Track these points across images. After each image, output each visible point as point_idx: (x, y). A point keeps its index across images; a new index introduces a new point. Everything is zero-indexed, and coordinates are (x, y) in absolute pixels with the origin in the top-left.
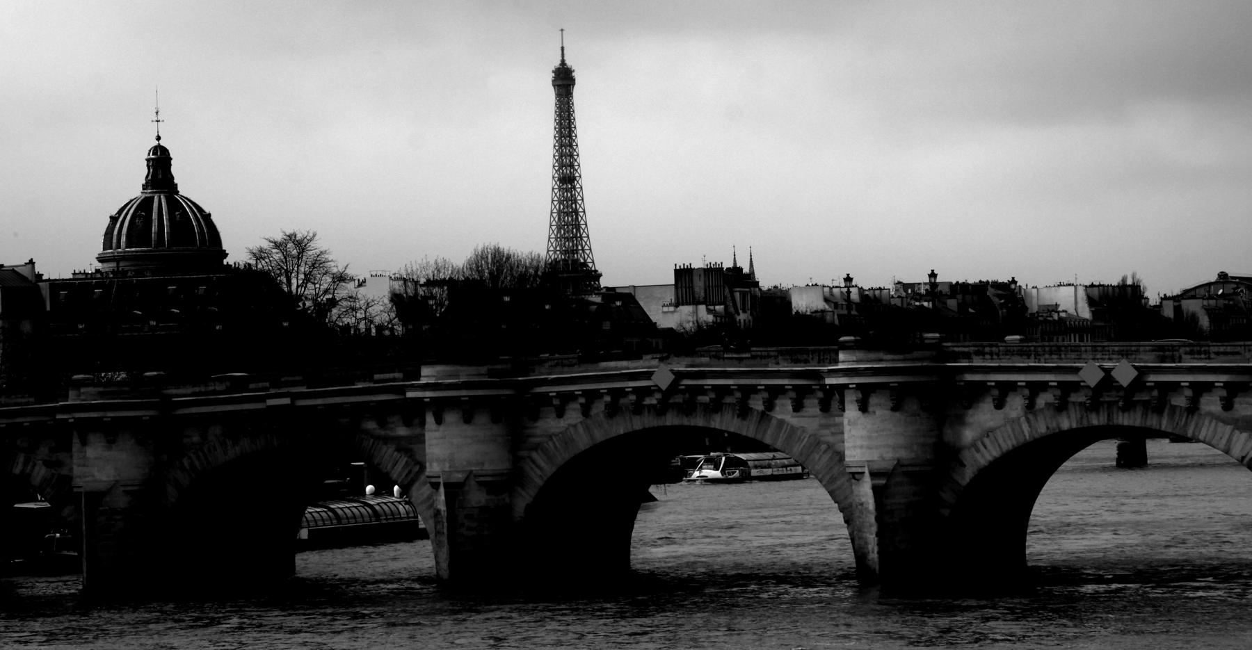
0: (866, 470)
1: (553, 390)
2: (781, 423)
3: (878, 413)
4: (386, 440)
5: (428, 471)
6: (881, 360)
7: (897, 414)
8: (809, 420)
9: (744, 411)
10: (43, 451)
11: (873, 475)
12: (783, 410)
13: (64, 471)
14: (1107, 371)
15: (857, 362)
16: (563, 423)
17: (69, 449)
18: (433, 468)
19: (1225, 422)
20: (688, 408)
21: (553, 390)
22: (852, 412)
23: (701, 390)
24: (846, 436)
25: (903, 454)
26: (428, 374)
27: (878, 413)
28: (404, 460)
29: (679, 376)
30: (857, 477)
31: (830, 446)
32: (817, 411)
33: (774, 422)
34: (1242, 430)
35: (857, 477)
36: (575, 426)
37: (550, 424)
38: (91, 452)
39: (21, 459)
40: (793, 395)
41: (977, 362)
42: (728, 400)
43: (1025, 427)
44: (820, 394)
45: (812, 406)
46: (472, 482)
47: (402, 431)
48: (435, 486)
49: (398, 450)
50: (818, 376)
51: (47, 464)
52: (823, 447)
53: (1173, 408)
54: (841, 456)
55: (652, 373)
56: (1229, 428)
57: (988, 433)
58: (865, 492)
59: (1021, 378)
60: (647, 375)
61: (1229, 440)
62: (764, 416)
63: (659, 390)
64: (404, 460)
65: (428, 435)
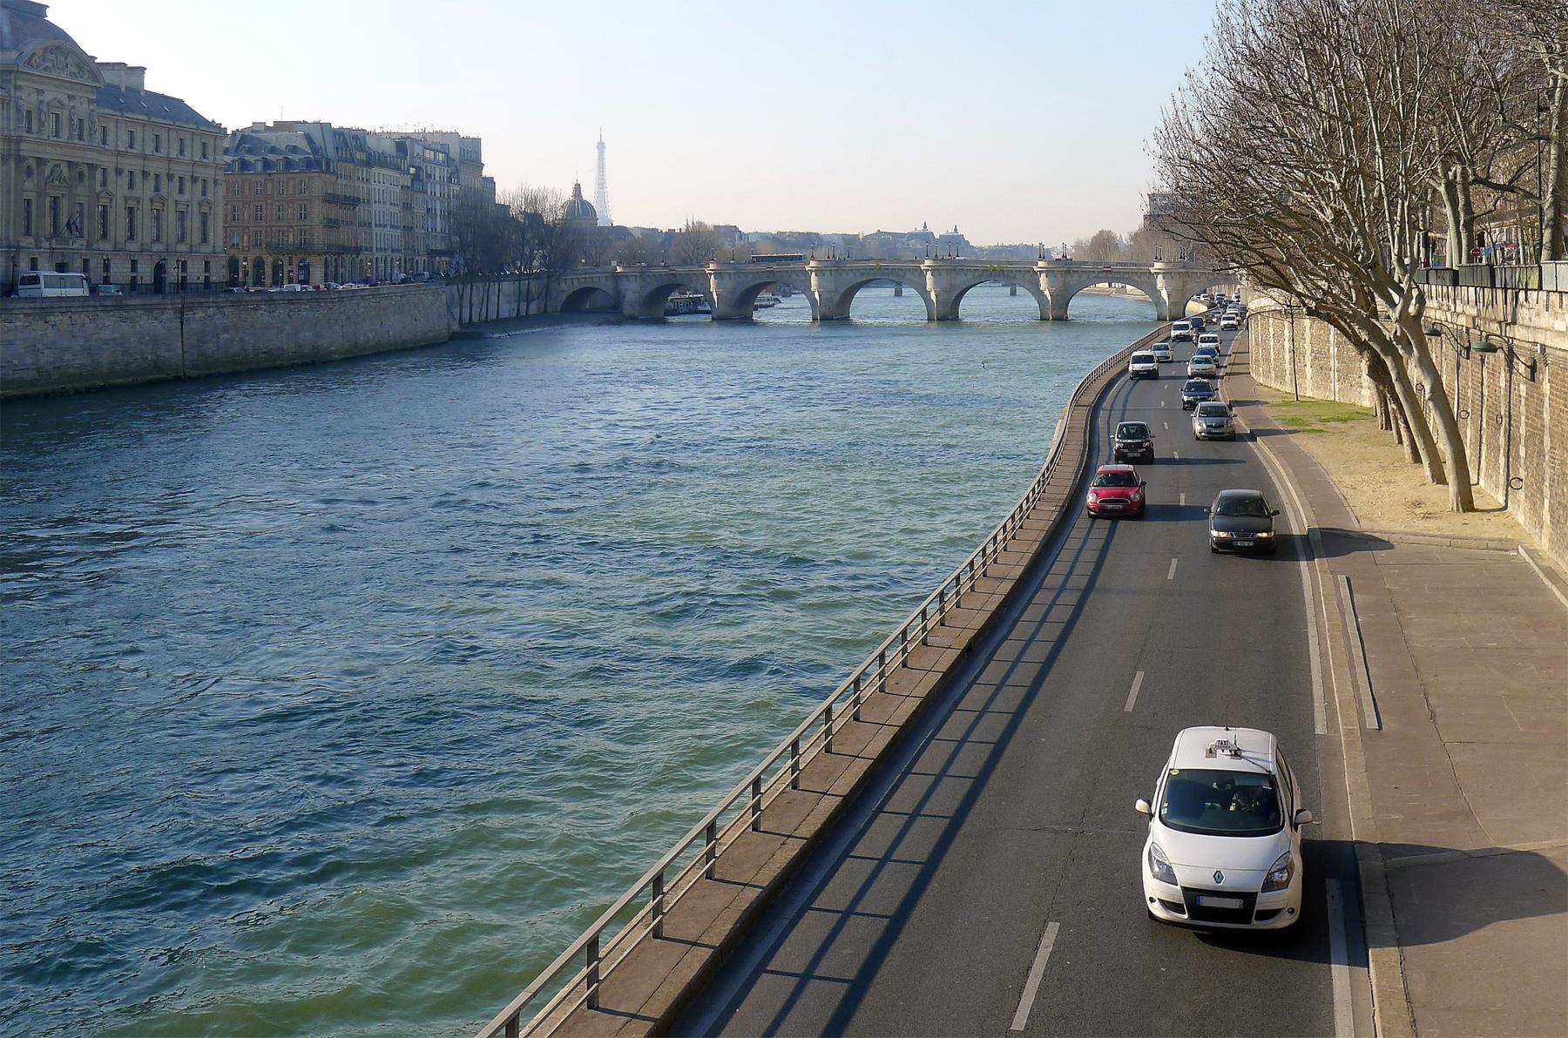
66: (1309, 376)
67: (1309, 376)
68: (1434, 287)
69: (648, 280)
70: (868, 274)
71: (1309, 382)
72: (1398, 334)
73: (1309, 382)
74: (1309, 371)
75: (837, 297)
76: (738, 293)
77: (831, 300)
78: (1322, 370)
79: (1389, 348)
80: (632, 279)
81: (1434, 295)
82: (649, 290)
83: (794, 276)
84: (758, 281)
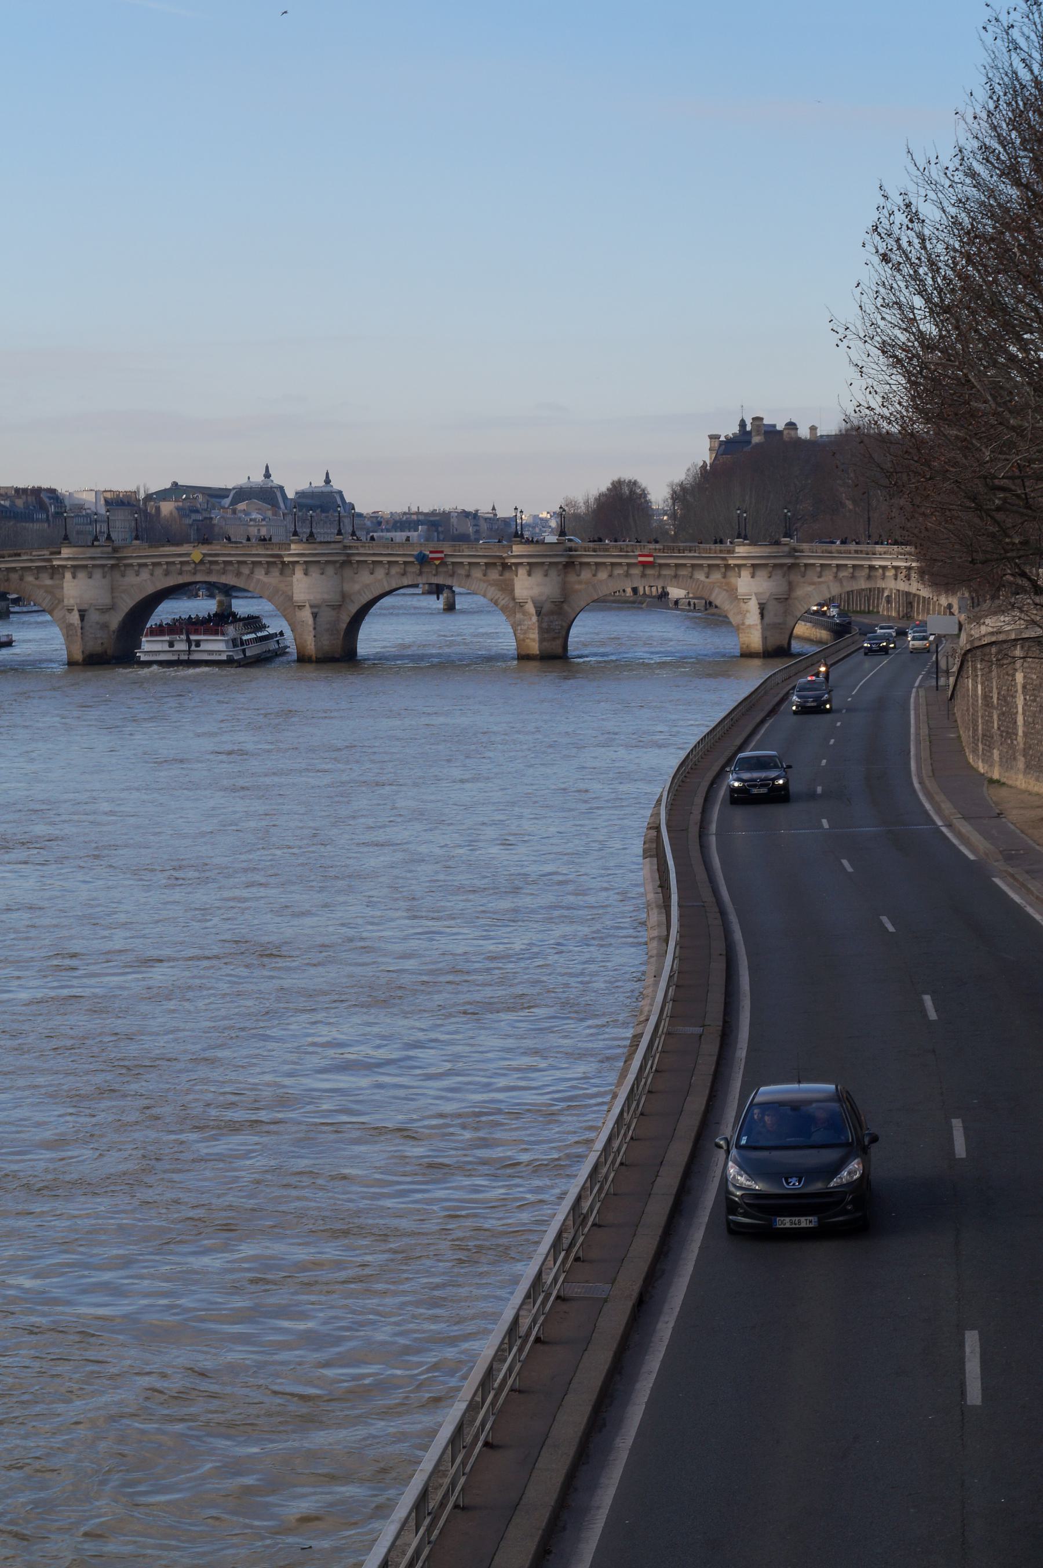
0: (307, 605)
1: (135, 562)
2: (258, 580)
3: (314, 575)
4: (39, 587)
5: (66, 602)
6: (316, 549)
7: (323, 576)
8: (273, 579)
9: (238, 574)
11: (312, 606)
12: (260, 574)
15: (303, 550)
16: (138, 579)
19: (484, 581)
20: (210, 572)
21: (135, 562)
23: (216, 562)
24: (295, 587)
25: (326, 596)
26: (66, 552)
27: (314, 575)
28: (50, 597)
29: (205, 555)
32: (278, 574)
33: (255, 580)
34: (492, 585)
36: (146, 581)
37: (131, 579)
40: (266, 566)
41: (362, 551)
42: (230, 568)
43: (385, 583)
44: (280, 566)
45: (275, 572)
47: (49, 582)
48: (70, 611)
49: (46, 592)
50: (279, 556)
52: (280, 593)
55: (190, 554)
56: (485, 585)
58: (306, 615)
59: (385, 559)
60: (188, 555)
61: (485, 591)
63: (194, 562)
64: (50, 597)
65: (65, 585)
70: (180, 573)
75: (115, 620)
77: (105, 626)
83: (30, 578)
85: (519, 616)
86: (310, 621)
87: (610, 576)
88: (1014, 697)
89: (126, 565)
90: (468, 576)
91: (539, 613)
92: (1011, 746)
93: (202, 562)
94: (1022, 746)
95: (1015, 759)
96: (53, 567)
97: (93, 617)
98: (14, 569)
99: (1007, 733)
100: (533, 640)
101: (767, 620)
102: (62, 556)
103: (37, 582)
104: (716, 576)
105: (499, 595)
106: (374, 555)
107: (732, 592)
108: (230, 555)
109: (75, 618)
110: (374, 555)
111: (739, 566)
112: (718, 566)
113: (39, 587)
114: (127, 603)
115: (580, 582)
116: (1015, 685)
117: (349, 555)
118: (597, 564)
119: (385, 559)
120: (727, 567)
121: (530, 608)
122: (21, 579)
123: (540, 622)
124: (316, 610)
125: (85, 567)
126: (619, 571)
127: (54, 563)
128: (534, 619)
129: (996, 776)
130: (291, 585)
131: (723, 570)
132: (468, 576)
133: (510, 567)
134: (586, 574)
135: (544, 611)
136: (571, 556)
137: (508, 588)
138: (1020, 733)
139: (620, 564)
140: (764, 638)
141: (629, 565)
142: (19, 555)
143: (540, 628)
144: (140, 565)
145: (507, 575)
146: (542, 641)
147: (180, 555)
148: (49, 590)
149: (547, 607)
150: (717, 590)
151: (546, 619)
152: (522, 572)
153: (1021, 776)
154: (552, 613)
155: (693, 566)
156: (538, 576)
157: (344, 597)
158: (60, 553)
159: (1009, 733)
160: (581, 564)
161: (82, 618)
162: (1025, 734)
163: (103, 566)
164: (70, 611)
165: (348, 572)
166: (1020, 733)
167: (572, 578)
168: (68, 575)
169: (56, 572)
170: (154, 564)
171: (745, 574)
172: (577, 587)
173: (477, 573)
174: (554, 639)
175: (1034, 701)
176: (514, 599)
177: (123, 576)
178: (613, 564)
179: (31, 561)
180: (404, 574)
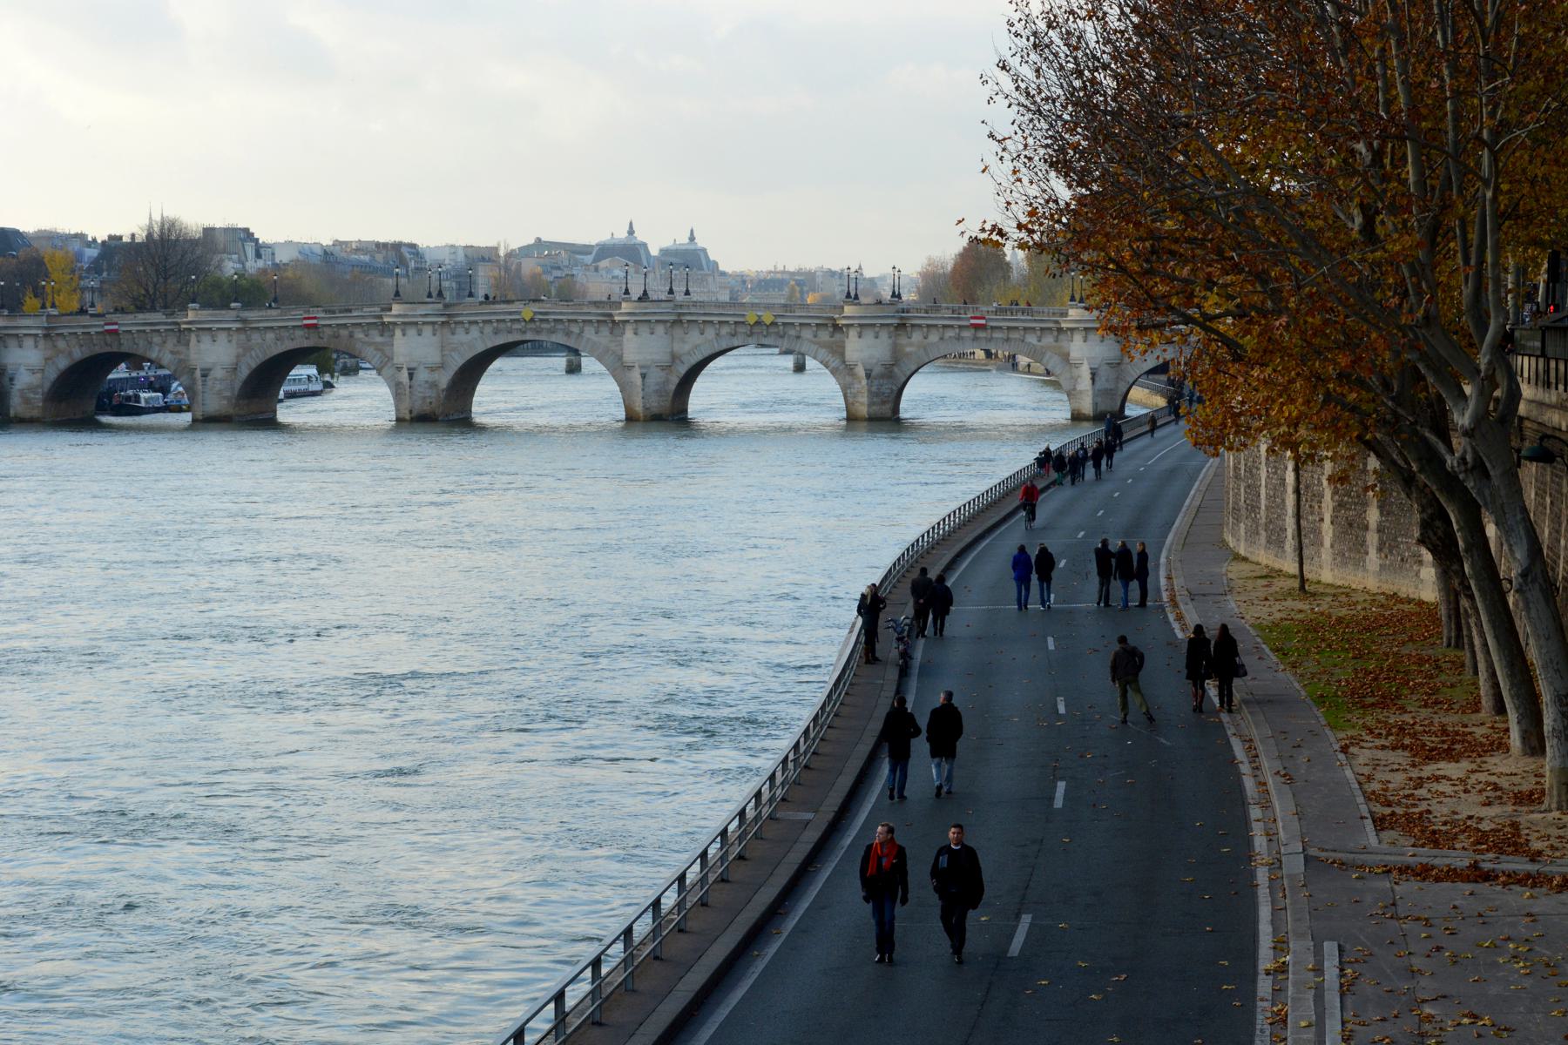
4: (370, 344)
5: (395, 361)
9: (568, 334)
10: (170, 345)
11: (641, 367)
12: (589, 332)
13: (182, 357)
14: (759, 317)
16: (469, 337)
17: (187, 344)
18: (399, 359)
19: (814, 343)
20: (538, 331)
22: (629, 334)
23: (547, 320)
29: (535, 313)
30: (630, 368)
31: (614, 352)
35: (630, 368)
37: (461, 336)
38: (202, 346)
39: (157, 348)
42: (560, 326)
45: (605, 330)
46: (422, 367)
47: (379, 339)
48: (399, 369)
49: (377, 349)
51: (172, 352)
53: (790, 336)
54: (620, 358)
57: (697, 347)
59: (715, 319)
60: (518, 313)
62: (580, 335)
66: (1327, 541)
67: (1327, 541)
68: (1553, 364)
69: (61, 344)
70: (510, 331)
71: (1326, 554)
72: (1469, 458)
73: (1326, 554)
74: (1327, 530)
75: (444, 379)
76: (244, 372)
77: (433, 385)
78: (1350, 528)
79: (1451, 483)
80: (29, 342)
81: (1553, 380)
82: (63, 363)
83: (359, 335)
84: (288, 345)
85: (848, 379)
86: (639, 381)
87: (942, 339)
88: (1258, 469)
89: (456, 323)
90: (798, 337)
91: (868, 376)
92: (1256, 521)
93: (532, 320)
94: (1264, 520)
95: (1258, 533)
96: (383, 323)
97: (422, 376)
98: (345, 325)
99: (1253, 506)
100: (862, 404)
101: (1099, 385)
102: (393, 312)
103: (367, 339)
104: (1048, 340)
105: (830, 358)
106: (705, 314)
107: (1065, 357)
108: (561, 313)
109: (404, 375)
110: (705, 314)
111: (1072, 330)
112: (1050, 329)
113: (370, 344)
114: (458, 361)
115: (911, 345)
116: (1259, 457)
117: (680, 314)
118: (928, 326)
119: (715, 319)
120: (1060, 330)
121: (861, 371)
122: (351, 336)
123: (870, 385)
124: (644, 371)
125: (416, 323)
126: (950, 333)
127: (386, 320)
128: (864, 382)
129: (1242, 552)
130: (621, 344)
131: (1055, 333)
132: (798, 337)
133: (841, 328)
134: (917, 336)
135: (873, 374)
136: (902, 318)
137: (838, 350)
138: (1263, 507)
139: (952, 326)
140: (1095, 404)
141: (960, 327)
142: (350, 311)
143: (870, 391)
144: (471, 323)
145: (838, 336)
146: (870, 405)
147: (510, 313)
148: (378, 348)
149: (877, 370)
150: (1049, 354)
151: (876, 382)
152: (853, 333)
153: (1262, 552)
154: (882, 376)
155: (1025, 329)
156: (869, 335)
157: (675, 358)
158: (390, 310)
159: (1253, 508)
160: (913, 326)
161: (411, 376)
162: (1267, 508)
163: (433, 323)
164: (399, 369)
165: (678, 332)
166: (1263, 507)
167: (903, 340)
168: (398, 333)
169: (386, 329)
170: (485, 322)
171: (1078, 338)
172: (908, 349)
173: (807, 334)
174: (883, 403)
175: (1275, 473)
176: (844, 362)
177: (453, 334)
178: (944, 326)
179: (363, 317)
180: (733, 335)
